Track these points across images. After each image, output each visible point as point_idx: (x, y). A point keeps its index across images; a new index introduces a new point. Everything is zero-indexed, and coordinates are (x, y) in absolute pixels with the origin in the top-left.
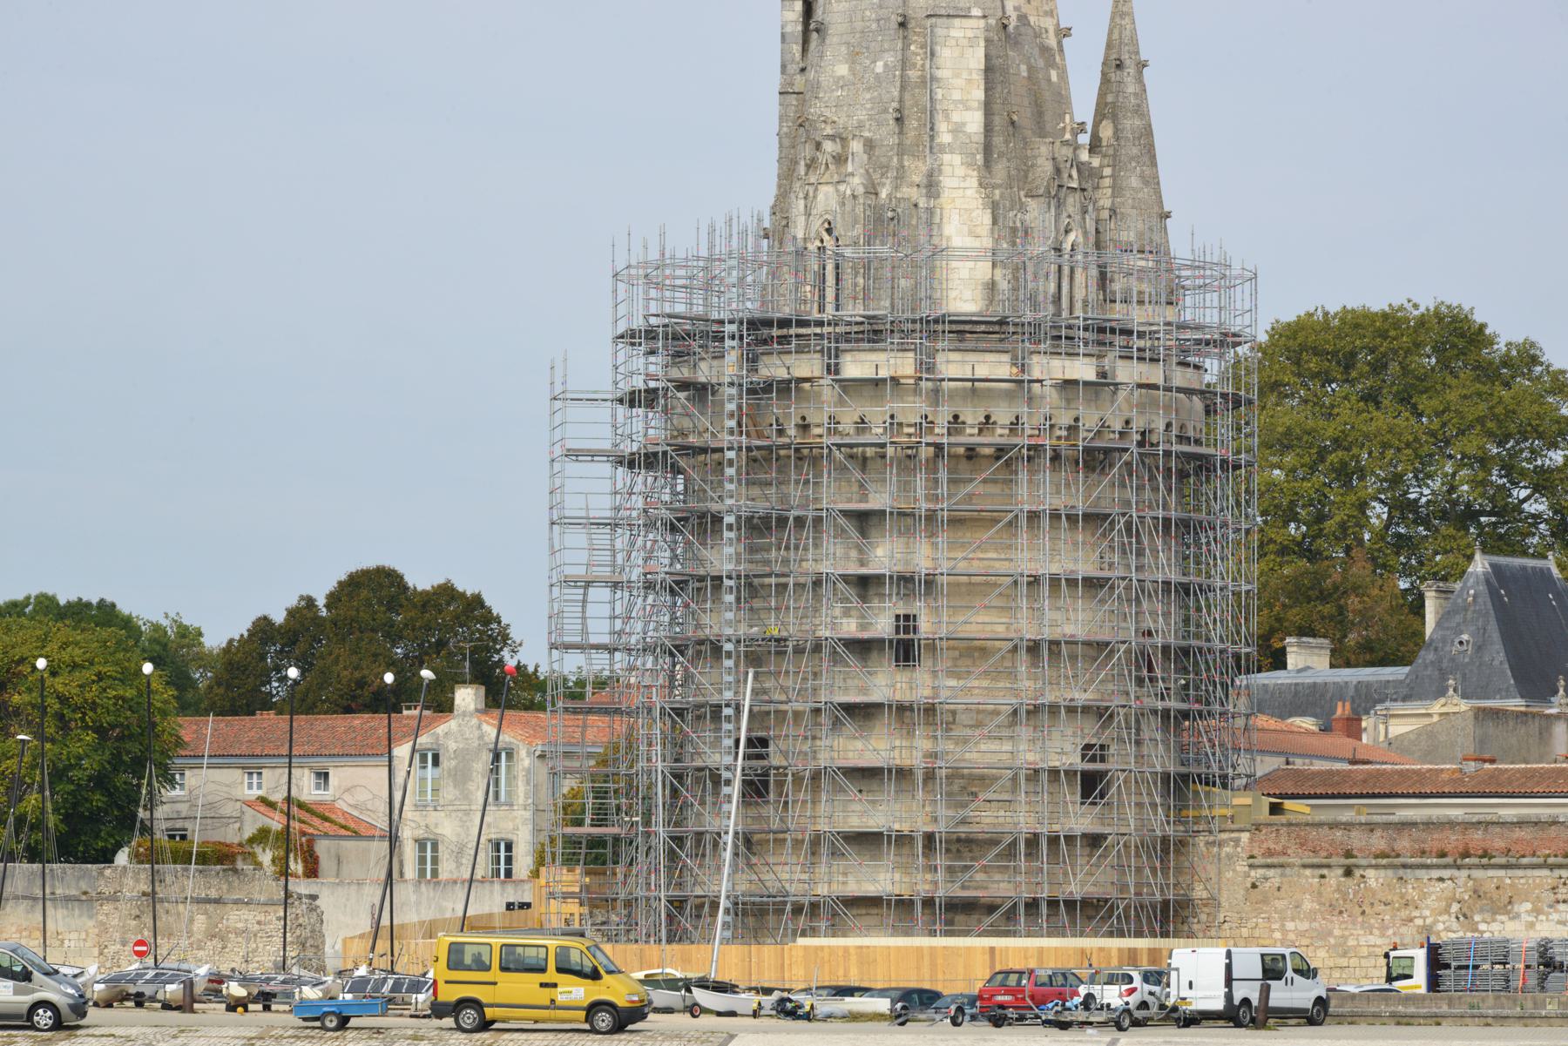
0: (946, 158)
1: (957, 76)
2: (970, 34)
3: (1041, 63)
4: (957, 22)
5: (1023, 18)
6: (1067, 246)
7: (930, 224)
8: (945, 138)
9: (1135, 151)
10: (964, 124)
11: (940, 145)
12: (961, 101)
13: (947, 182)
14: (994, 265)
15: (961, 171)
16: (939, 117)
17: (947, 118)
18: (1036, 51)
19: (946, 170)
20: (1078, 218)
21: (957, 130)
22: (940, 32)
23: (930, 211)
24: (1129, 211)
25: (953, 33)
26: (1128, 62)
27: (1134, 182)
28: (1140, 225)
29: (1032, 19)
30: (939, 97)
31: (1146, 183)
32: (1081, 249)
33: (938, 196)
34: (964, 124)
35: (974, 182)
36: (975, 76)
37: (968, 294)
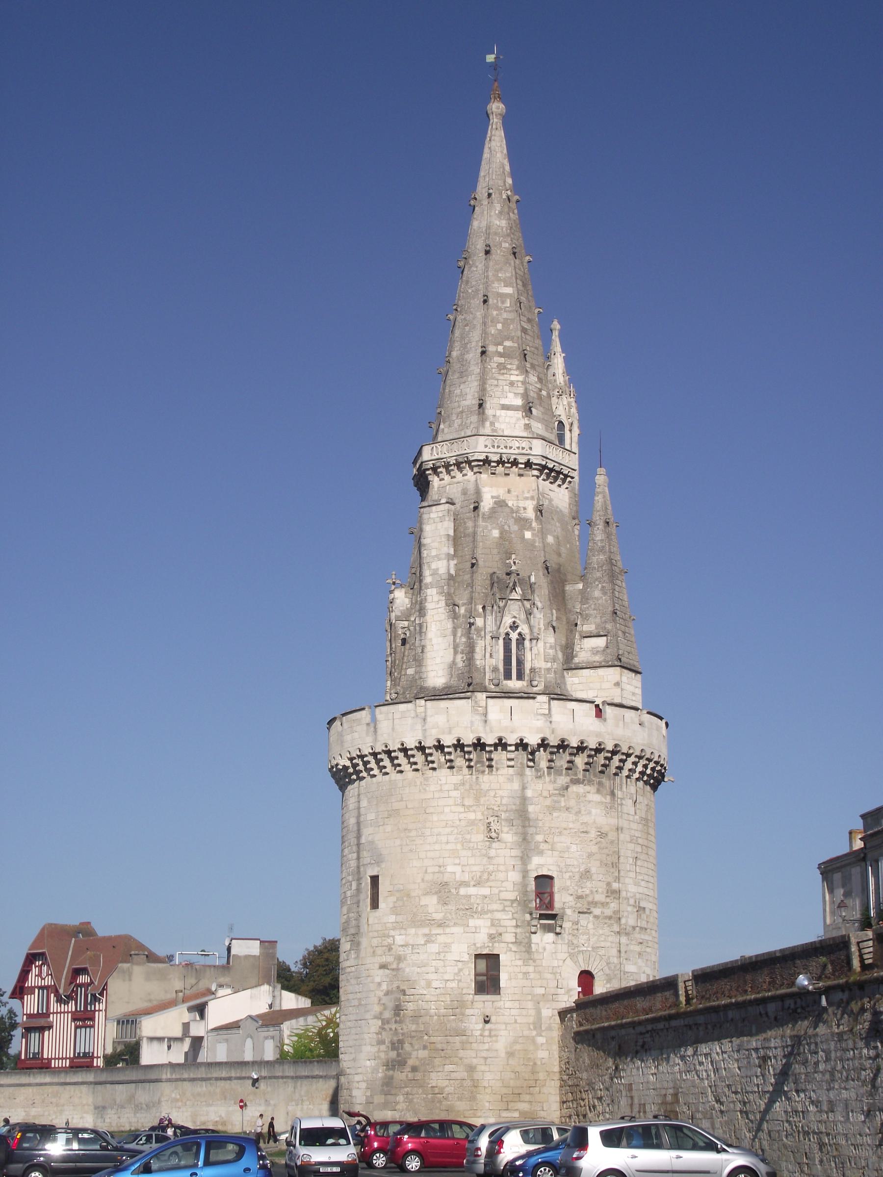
0: (429, 592)
1: (433, 542)
2: (440, 514)
3: (515, 528)
4: (434, 508)
5: (500, 504)
6: (514, 636)
7: (421, 632)
8: (428, 579)
9: (599, 574)
10: (438, 569)
11: (426, 584)
12: (436, 556)
13: (429, 605)
14: (456, 653)
15: (436, 598)
16: (425, 567)
17: (429, 566)
18: (511, 522)
19: (429, 599)
20: (523, 616)
21: (435, 573)
22: (425, 516)
23: (421, 625)
24: (592, 612)
25: (432, 515)
26: (598, 522)
27: (597, 593)
28: (598, 620)
29: (510, 504)
30: (425, 555)
31: (605, 594)
32: (528, 637)
33: (424, 615)
34: (438, 569)
35: (443, 603)
36: (443, 539)
37: (441, 673)
